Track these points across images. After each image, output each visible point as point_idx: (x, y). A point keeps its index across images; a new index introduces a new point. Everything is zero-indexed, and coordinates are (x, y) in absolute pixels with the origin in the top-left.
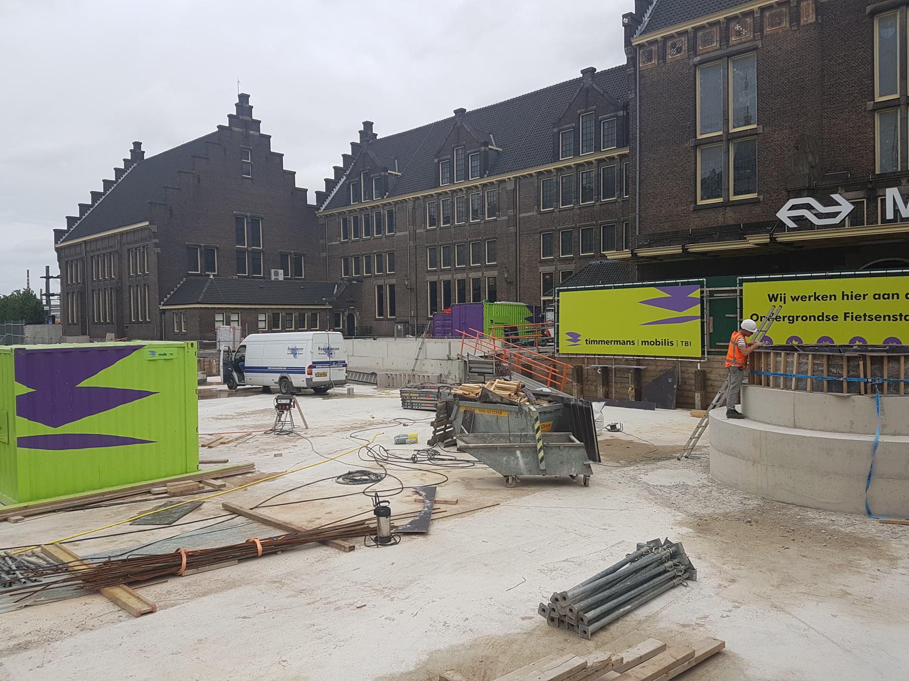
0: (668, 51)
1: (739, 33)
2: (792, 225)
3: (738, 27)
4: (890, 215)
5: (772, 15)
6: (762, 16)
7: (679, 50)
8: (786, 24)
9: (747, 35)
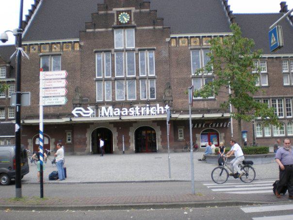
0: (31, 49)
1: (55, 48)
2: (76, 115)
3: (55, 46)
4: (103, 114)
6: (63, 45)
7: (35, 50)
8: (70, 49)
9: (58, 49)
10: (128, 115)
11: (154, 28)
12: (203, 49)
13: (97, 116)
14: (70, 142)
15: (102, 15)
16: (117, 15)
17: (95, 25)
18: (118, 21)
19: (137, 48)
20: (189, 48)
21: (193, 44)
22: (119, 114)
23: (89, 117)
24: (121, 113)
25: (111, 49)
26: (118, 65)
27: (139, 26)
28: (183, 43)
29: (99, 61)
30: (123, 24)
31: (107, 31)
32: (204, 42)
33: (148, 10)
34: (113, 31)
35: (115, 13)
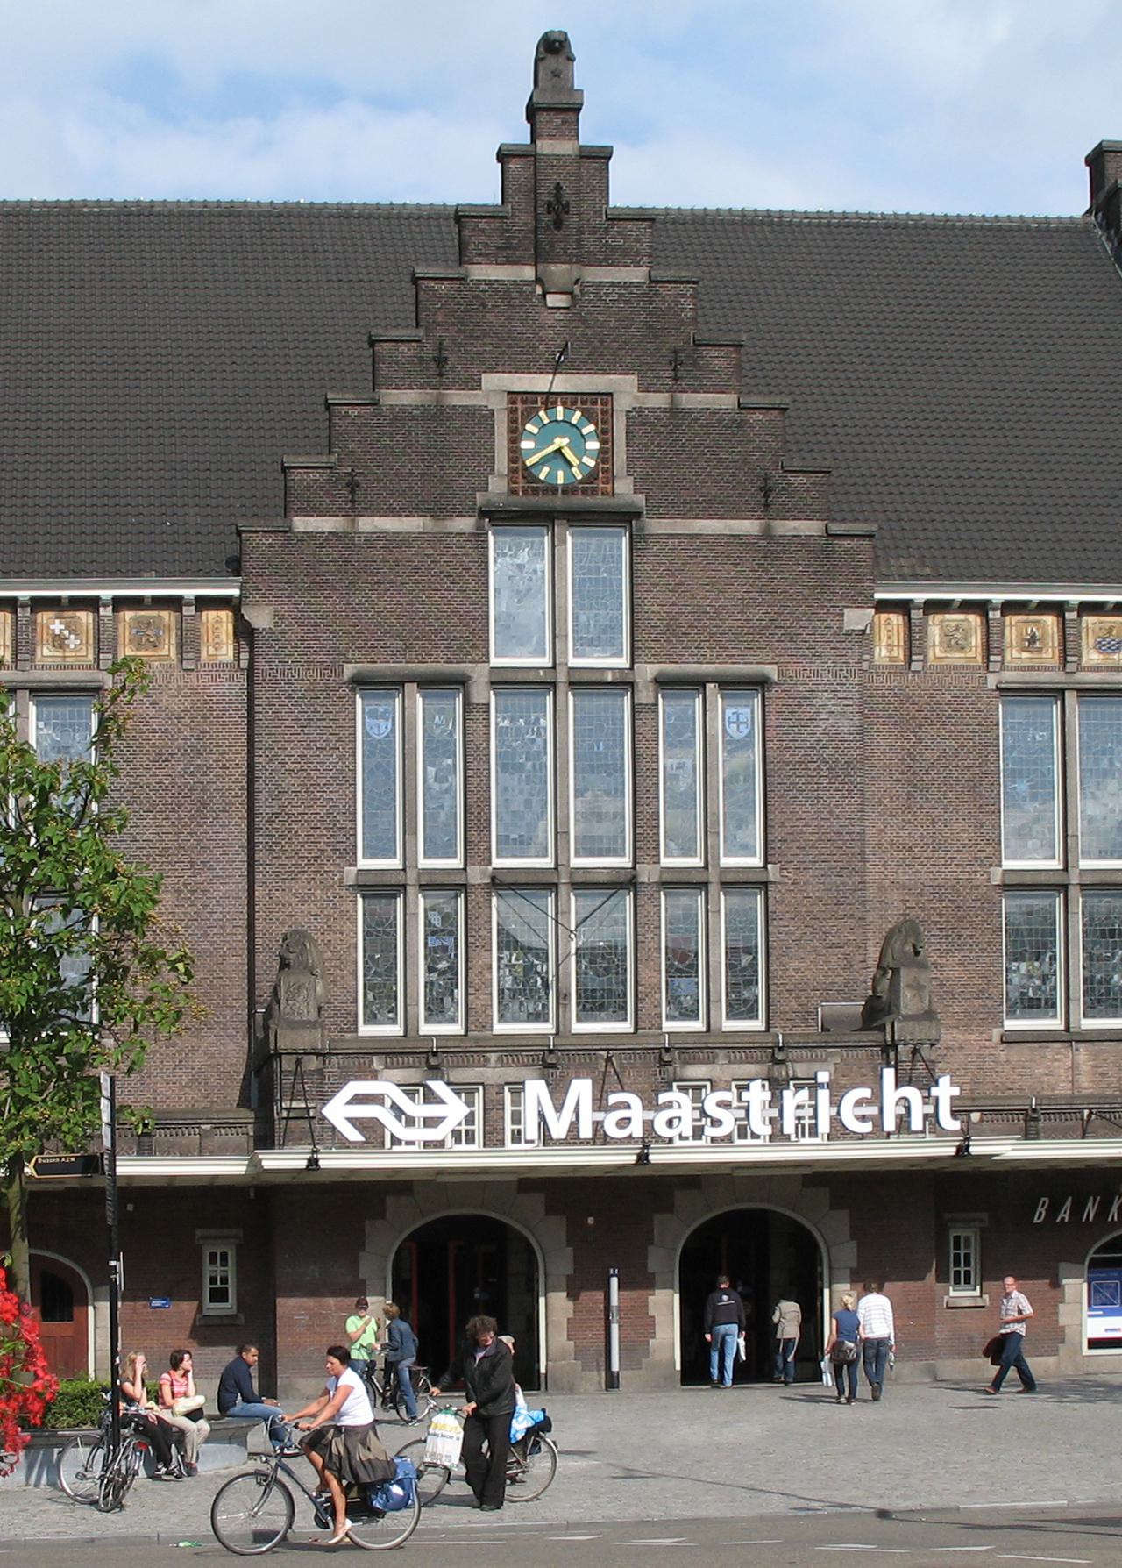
2: (353, 1135)
4: (531, 1130)
5: (138, 621)
8: (169, 649)
10: (698, 1132)
11: (767, 534)
12: (1084, 692)
13: (493, 1138)
14: (230, 1306)
15: (403, 415)
16: (512, 421)
17: (353, 486)
18: (520, 471)
19: (648, 671)
20: (992, 681)
21: (1014, 655)
22: (636, 1130)
23: (441, 1144)
24: (649, 1126)
25: (465, 667)
26: (513, 781)
27: (657, 511)
28: (953, 641)
29: (379, 750)
30: (552, 489)
31: (439, 538)
32: (1088, 641)
33: (727, 400)
34: (479, 537)
35: (499, 405)
